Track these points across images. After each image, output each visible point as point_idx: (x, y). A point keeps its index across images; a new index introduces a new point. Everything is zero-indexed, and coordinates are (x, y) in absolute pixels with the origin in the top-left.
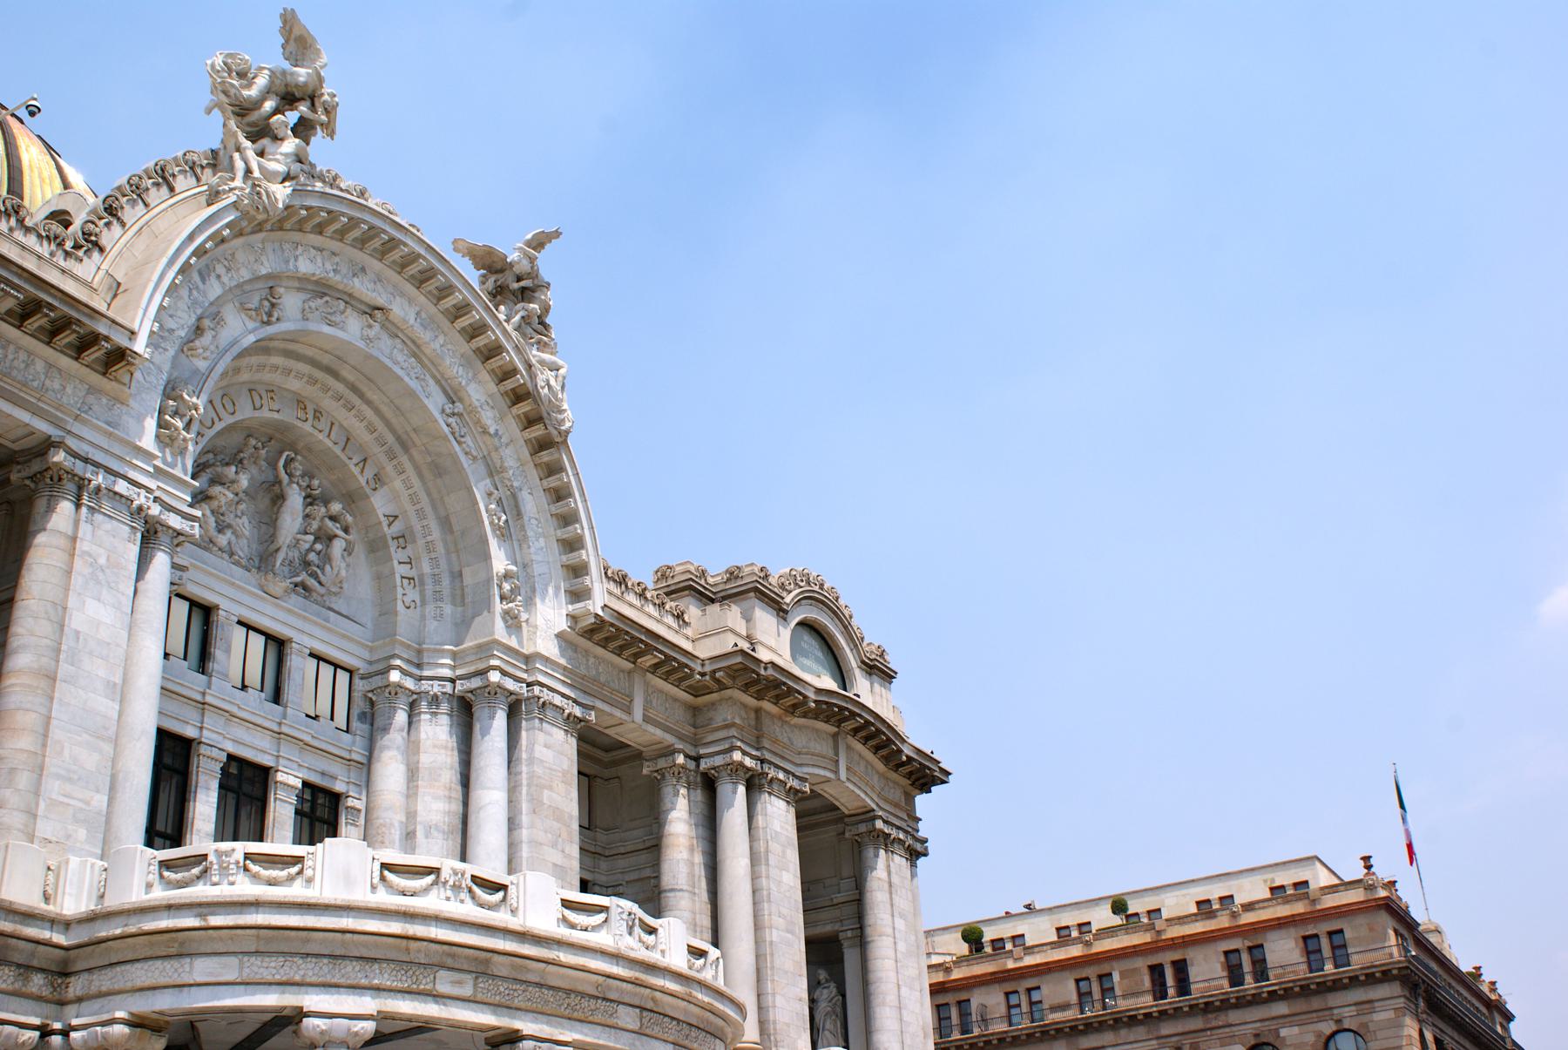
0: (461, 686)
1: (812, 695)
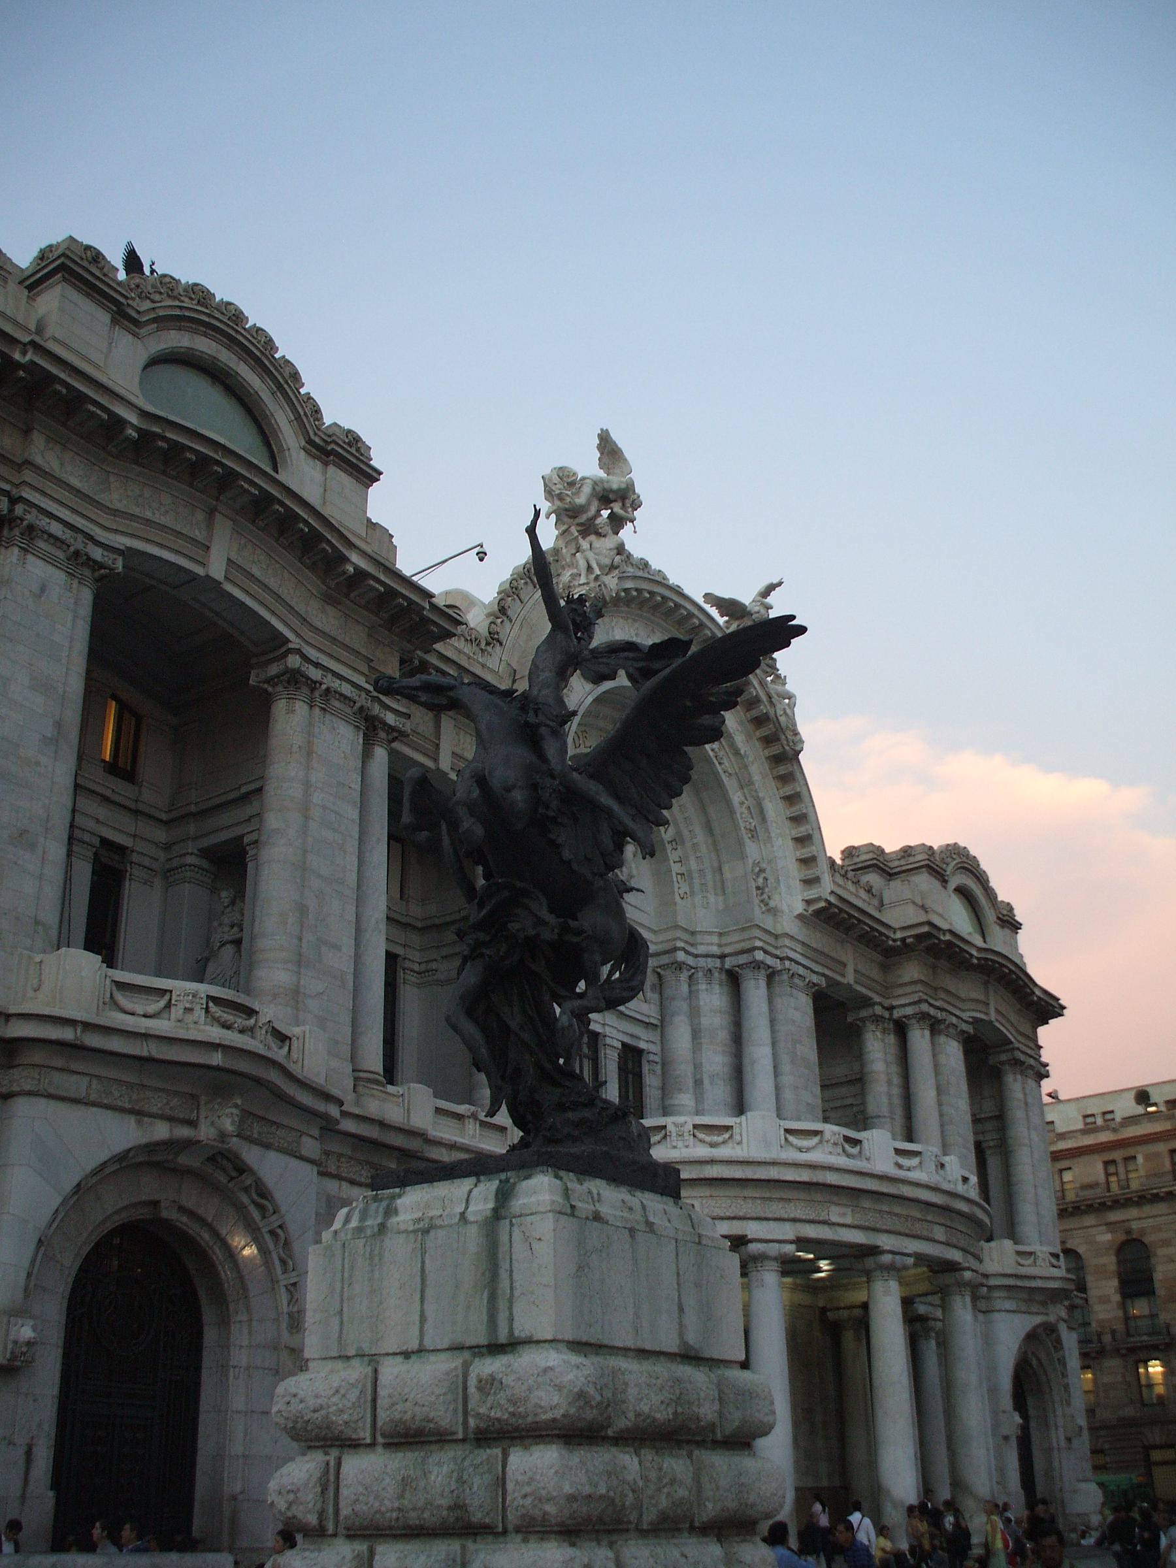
0: (729, 962)
1: (974, 953)
